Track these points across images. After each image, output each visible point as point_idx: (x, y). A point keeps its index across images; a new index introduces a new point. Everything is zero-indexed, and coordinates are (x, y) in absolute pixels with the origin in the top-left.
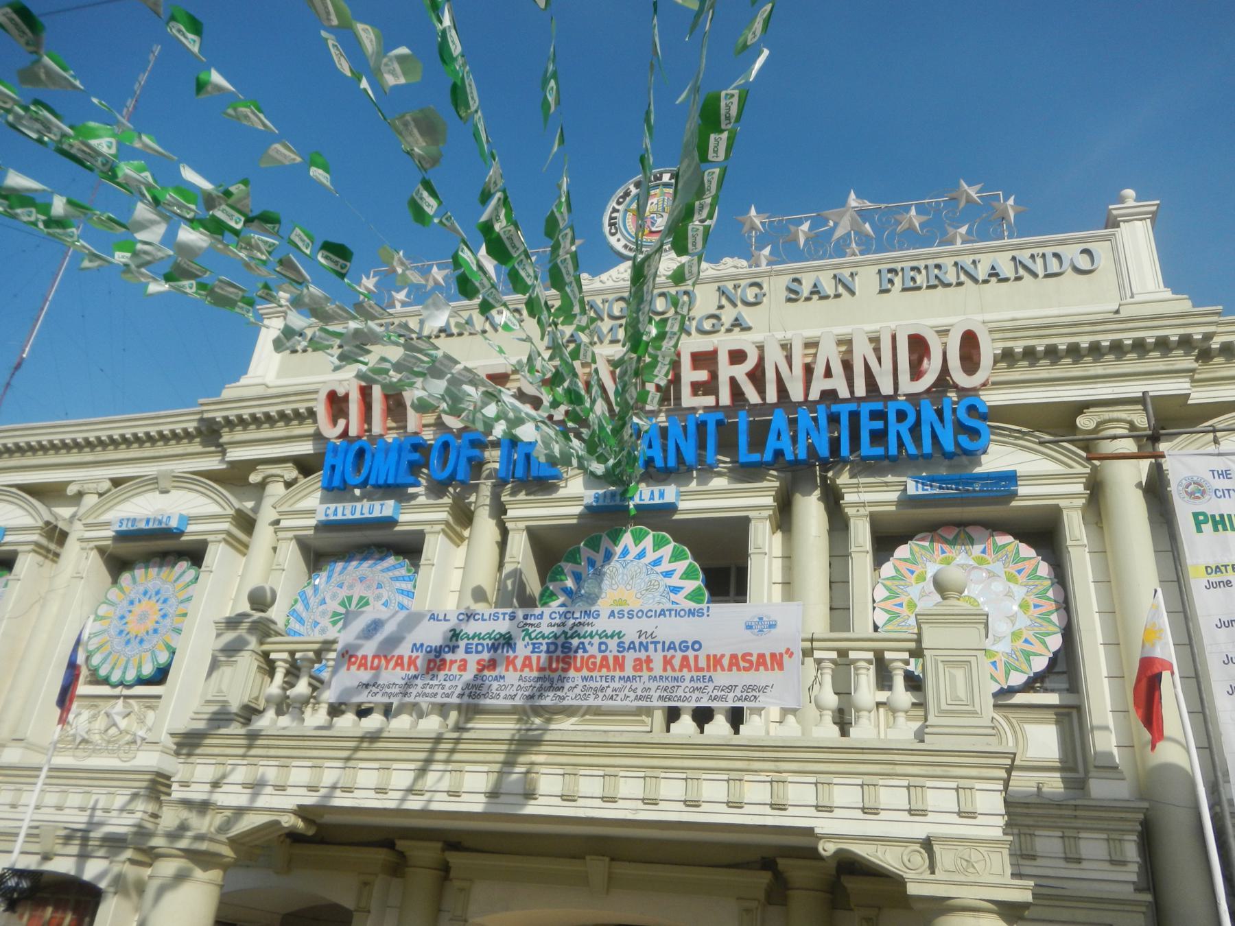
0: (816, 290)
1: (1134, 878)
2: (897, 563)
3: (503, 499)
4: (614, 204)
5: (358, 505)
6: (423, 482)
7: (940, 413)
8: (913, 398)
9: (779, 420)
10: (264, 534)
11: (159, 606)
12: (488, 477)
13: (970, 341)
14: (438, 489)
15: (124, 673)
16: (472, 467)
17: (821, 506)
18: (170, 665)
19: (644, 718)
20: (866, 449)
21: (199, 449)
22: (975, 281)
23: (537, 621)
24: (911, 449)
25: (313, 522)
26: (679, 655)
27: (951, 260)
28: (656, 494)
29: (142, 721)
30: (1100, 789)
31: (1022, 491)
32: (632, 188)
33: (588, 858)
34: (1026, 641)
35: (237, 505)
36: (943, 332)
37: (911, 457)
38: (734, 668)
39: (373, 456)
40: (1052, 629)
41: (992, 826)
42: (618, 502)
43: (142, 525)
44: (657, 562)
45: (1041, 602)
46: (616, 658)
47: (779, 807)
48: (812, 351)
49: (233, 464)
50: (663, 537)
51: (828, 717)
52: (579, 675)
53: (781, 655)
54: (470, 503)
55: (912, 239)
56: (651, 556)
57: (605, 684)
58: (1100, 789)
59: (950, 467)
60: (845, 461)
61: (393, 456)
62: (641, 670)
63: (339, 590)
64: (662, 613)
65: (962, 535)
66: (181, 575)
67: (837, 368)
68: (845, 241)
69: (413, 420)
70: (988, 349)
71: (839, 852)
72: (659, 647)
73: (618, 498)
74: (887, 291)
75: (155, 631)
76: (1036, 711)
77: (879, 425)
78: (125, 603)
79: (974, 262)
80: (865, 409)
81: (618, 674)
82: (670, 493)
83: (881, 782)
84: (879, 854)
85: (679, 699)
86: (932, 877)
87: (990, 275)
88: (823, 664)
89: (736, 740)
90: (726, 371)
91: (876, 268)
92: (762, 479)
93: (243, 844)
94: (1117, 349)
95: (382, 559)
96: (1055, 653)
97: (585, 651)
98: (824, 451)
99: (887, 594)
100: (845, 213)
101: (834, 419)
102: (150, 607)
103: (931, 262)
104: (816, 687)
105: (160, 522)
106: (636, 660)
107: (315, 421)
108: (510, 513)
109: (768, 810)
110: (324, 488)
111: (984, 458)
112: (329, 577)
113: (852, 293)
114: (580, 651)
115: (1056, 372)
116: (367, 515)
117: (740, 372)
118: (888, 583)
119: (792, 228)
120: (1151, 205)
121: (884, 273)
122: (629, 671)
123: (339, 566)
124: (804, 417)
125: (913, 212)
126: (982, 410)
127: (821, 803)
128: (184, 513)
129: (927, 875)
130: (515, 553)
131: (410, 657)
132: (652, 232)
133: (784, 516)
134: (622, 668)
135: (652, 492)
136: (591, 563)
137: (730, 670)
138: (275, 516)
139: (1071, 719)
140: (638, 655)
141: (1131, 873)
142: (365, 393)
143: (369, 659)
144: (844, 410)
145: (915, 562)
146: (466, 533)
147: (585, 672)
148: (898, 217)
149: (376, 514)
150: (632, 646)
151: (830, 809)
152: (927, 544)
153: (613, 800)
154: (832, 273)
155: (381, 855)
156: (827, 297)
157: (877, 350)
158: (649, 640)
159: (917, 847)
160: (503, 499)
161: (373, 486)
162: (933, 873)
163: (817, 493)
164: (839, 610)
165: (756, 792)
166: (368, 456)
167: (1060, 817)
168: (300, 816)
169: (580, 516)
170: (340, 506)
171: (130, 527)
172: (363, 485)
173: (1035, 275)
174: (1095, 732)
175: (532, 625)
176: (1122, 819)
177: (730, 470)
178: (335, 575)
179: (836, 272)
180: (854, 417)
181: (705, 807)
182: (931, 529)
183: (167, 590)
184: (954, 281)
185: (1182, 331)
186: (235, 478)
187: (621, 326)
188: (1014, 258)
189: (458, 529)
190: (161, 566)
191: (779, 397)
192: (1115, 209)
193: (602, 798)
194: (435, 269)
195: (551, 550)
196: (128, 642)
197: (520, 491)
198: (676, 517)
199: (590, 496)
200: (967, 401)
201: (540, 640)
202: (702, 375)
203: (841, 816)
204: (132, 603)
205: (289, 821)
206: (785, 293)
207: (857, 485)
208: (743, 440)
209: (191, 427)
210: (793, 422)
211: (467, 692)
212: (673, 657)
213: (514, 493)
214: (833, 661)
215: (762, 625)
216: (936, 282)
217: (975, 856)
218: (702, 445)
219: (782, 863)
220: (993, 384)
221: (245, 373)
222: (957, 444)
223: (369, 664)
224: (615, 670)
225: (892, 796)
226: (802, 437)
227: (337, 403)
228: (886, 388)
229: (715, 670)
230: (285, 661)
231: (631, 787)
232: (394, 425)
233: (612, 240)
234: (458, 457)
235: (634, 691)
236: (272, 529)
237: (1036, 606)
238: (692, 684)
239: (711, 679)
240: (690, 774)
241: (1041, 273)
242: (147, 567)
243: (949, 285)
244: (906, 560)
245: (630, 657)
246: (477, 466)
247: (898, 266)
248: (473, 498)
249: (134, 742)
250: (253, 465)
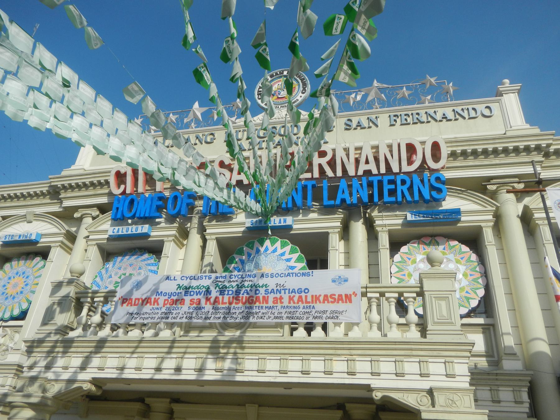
0: (359, 125)
1: (527, 410)
2: (402, 255)
3: (204, 224)
5: (130, 227)
6: (164, 216)
7: (422, 181)
8: (408, 173)
9: (343, 184)
10: (80, 243)
11: (24, 280)
12: (197, 213)
13: (436, 146)
14: (171, 219)
15: (4, 314)
16: (189, 209)
17: (364, 227)
18: (28, 309)
19: (279, 329)
20: (387, 198)
21: (49, 201)
22: (436, 120)
24: (409, 198)
25: (107, 236)
26: (297, 295)
27: (424, 111)
28: (282, 221)
29: (12, 339)
30: (508, 365)
31: (463, 219)
33: (247, 405)
34: (467, 292)
35: (67, 228)
36: (423, 143)
37: (408, 202)
38: (326, 302)
39: (138, 203)
40: (479, 286)
41: (464, 382)
42: (263, 225)
43: (17, 238)
44: (283, 254)
45: (474, 273)
46: (264, 297)
47: (351, 373)
48: (359, 152)
49: (65, 208)
50: (286, 242)
51: (375, 327)
53: (350, 295)
54: (188, 227)
55: (404, 101)
56: (280, 251)
57: (258, 311)
58: (508, 365)
59: (427, 207)
60: (376, 205)
61: (149, 202)
62: (277, 303)
63: (118, 271)
64: (289, 275)
65: (433, 241)
66: (36, 264)
67: (371, 159)
68: (372, 102)
69: (159, 186)
70: (445, 151)
71: (384, 397)
72: (287, 291)
73: (263, 223)
74: (394, 125)
75: (21, 292)
76: (473, 327)
77: (392, 187)
78: (6, 278)
79: (435, 112)
80: (386, 179)
81: (265, 305)
82: (289, 220)
83: (405, 360)
84: (405, 398)
85: (297, 318)
86: (434, 409)
87: (443, 118)
88: (372, 300)
89: (328, 339)
91: (388, 115)
92: (334, 214)
93: (61, 400)
94: (506, 151)
95: (142, 255)
96: (481, 298)
98: (366, 199)
99: (397, 270)
100: (372, 90)
101: (370, 185)
102: (20, 280)
103: (414, 112)
104: (368, 312)
105: (26, 237)
106: (274, 298)
107: (109, 187)
108: (208, 231)
109: (346, 375)
110: (112, 219)
111: (443, 203)
112: (114, 264)
113: (377, 126)
114: (245, 294)
115: (477, 163)
116: (135, 232)
117: (324, 161)
118: (398, 264)
119: (347, 96)
120: (518, 86)
121: (392, 117)
122: (271, 304)
123: (119, 258)
124: (355, 183)
125: (405, 89)
126: (442, 179)
127: (374, 372)
128: (40, 232)
129: (431, 408)
130: (210, 251)
131: (155, 299)
132: (278, 98)
133: (345, 232)
134: (267, 302)
135: (280, 220)
136: (249, 255)
137: (324, 302)
138: (87, 234)
139: (491, 331)
140: (275, 295)
141: (525, 408)
142: (135, 172)
143: (133, 300)
144: (375, 180)
145: (411, 254)
146: (185, 242)
148: (397, 92)
149: (139, 231)
151: (379, 374)
152: (416, 245)
153: (263, 371)
154: (367, 117)
155: (138, 406)
156: (364, 128)
157: (391, 151)
158: (282, 288)
159: (425, 394)
160: (204, 224)
161: (138, 218)
162: (434, 407)
163: (362, 220)
164: (374, 276)
165: (339, 366)
166: (135, 203)
167: (489, 379)
168: (93, 384)
169: (243, 232)
170: (120, 228)
171: (10, 239)
172: (133, 217)
173: (464, 118)
174: (504, 336)
176: (520, 380)
177: (319, 209)
178: (117, 263)
180: (380, 183)
181: (312, 374)
182: (419, 238)
183: (29, 271)
184: (426, 121)
185: (536, 143)
186: (67, 215)
187: (264, 141)
188: (454, 110)
189: (181, 240)
190: (26, 260)
192: (501, 88)
193: (257, 371)
194: (171, 115)
195: (229, 251)
196: (7, 298)
197: (212, 220)
198: (292, 232)
199: (249, 222)
200: (435, 175)
201: (224, 289)
203: (385, 379)
204: (10, 278)
205: (87, 386)
206: (344, 126)
207: (382, 216)
208: (325, 194)
209: (45, 190)
210: (350, 186)
211: (185, 316)
212: (294, 296)
213: (210, 221)
214: (378, 299)
215: (340, 280)
216: (417, 121)
217: (456, 398)
218: (305, 197)
219: (348, 406)
220: (447, 168)
221: (74, 163)
222: (431, 196)
223: (133, 303)
224: (263, 303)
225: (411, 367)
226: (354, 192)
227: (120, 177)
228: (395, 169)
229: (316, 303)
230: (89, 303)
231: (272, 365)
232: (149, 188)
234: (182, 203)
235: (273, 314)
236: (85, 240)
237: (471, 275)
239: (314, 307)
240: (305, 357)
241: (467, 117)
242: (19, 260)
243: (423, 122)
244: (406, 253)
245: (271, 297)
246: (191, 208)
247: (399, 114)
248: (189, 225)
249: (7, 350)
250: (76, 208)
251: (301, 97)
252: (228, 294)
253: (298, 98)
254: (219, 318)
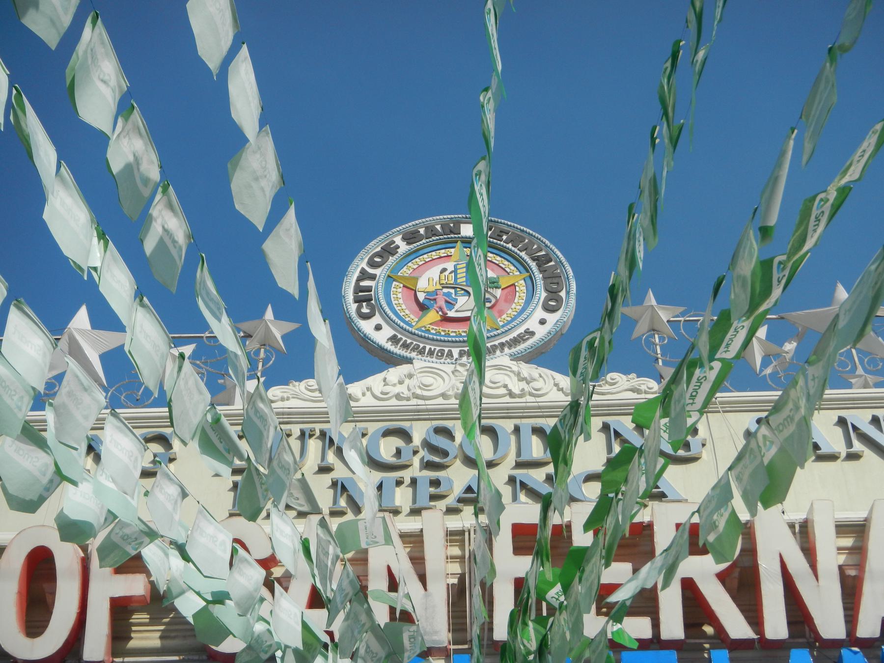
4: (364, 265)
32: (398, 240)
132: (446, 319)
179: (843, 413)
187: (399, 483)
191: (792, 623)
233: (366, 327)
251: (543, 322)
253: (532, 324)
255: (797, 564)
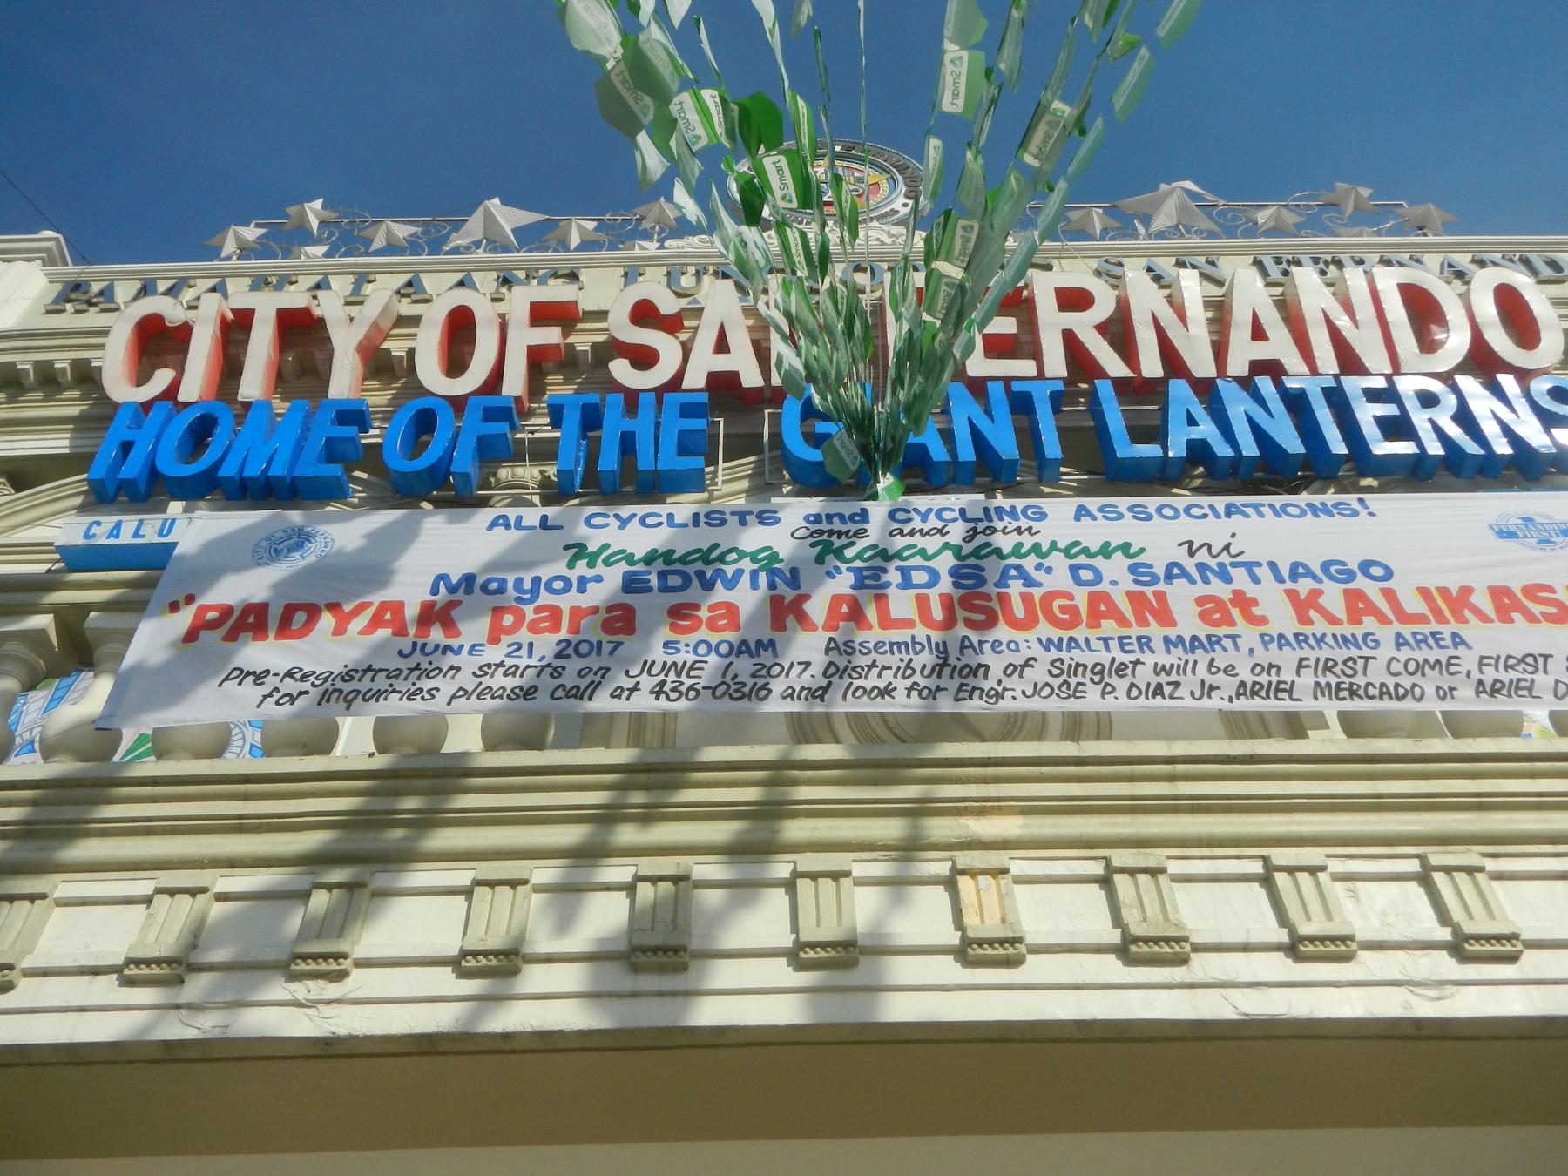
23: (853, 527)
52: (1031, 635)
85: (1384, 692)
90: (1051, 322)
97: (1030, 582)
117: (1084, 324)
147: (1045, 629)
150: (1173, 571)
175: (840, 534)
202: (1005, 325)
218: (1029, 436)
238: (1404, 654)
239: (1458, 640)
245: (1181, 597)
251: (905, 205)
252: (906, 583)
254: (887, 692)
255: (1167, 316)
